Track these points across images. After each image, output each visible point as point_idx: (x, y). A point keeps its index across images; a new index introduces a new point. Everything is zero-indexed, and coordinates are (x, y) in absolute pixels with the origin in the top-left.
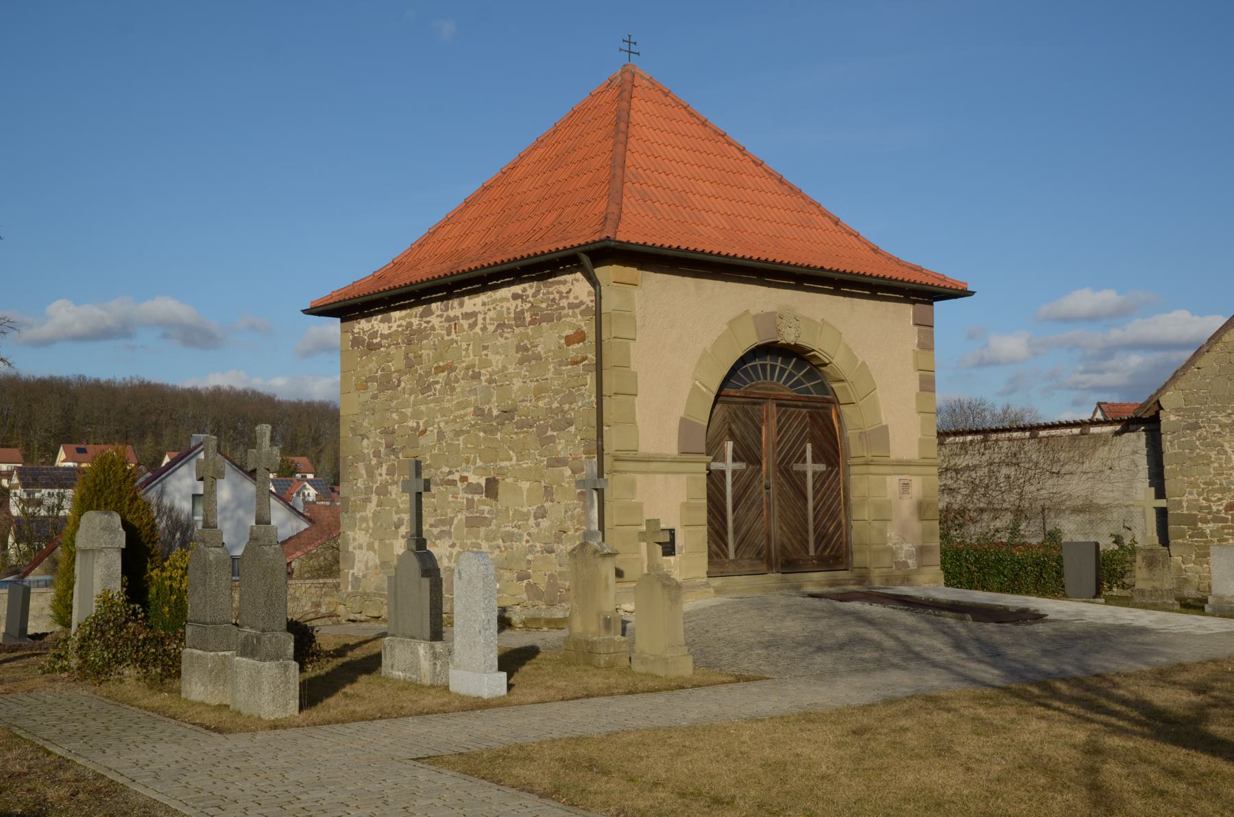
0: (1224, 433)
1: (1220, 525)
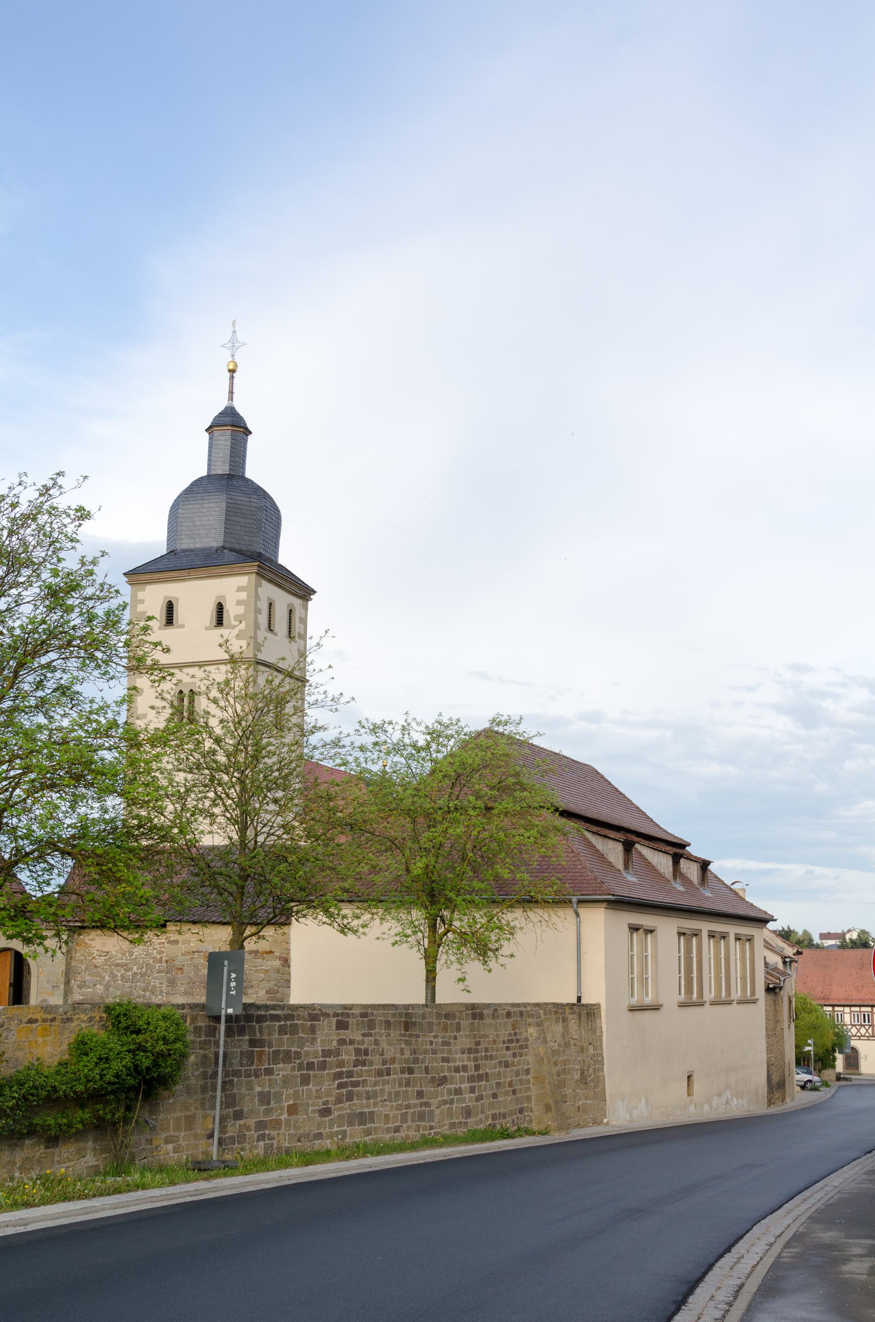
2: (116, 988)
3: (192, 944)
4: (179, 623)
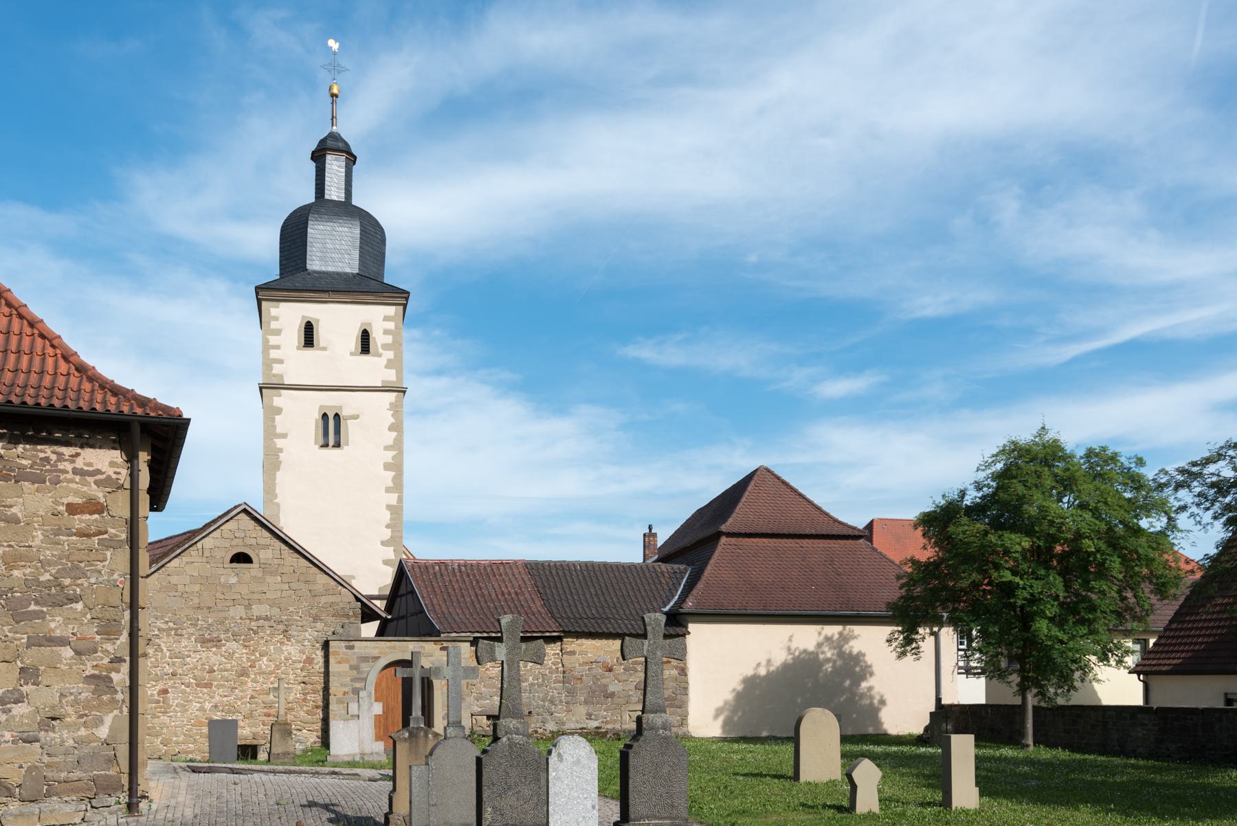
0: (161, 636)
1: (154, 705)
4: (321, 346)
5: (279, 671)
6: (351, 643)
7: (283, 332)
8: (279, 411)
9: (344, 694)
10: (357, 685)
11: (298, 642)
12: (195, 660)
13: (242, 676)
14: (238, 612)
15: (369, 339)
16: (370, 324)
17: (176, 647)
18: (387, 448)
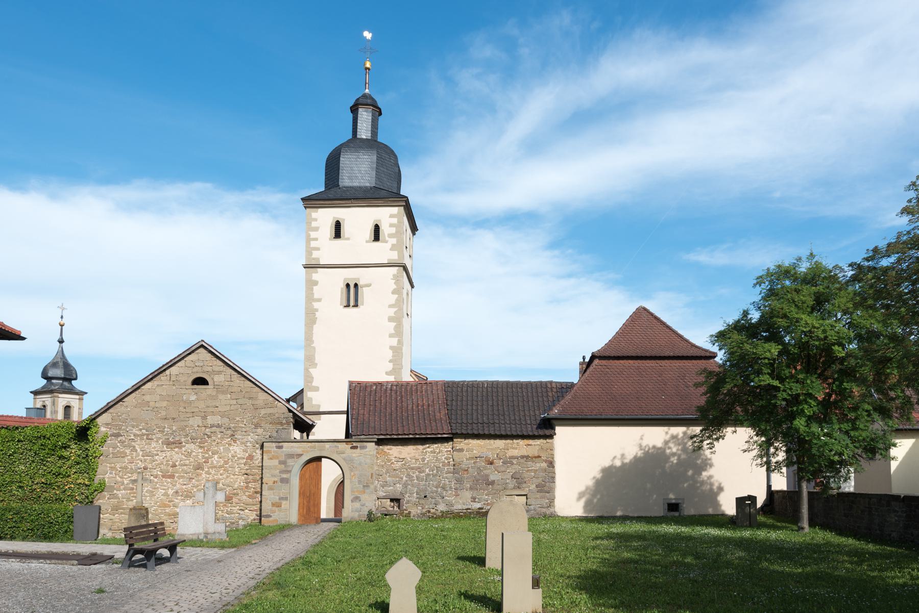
2: (413, 486)
3: (475, 452)
4: (346, 237)
5: (227, 466)
6: (281, 444)
7: (320, 229)
8: (316, 283)
9: (274, 483)
10: (285, 476)
11: (242, 443)
12: (161, 458)
13: (198, 469)
14: (196, 421)
15: (379, 231)
16: (380, 220)
17: (147, 448)
18: (390, 306)
